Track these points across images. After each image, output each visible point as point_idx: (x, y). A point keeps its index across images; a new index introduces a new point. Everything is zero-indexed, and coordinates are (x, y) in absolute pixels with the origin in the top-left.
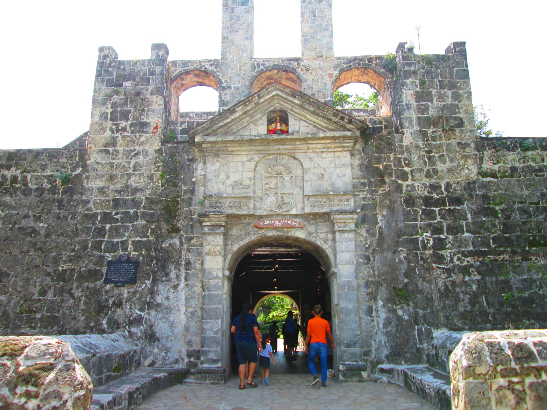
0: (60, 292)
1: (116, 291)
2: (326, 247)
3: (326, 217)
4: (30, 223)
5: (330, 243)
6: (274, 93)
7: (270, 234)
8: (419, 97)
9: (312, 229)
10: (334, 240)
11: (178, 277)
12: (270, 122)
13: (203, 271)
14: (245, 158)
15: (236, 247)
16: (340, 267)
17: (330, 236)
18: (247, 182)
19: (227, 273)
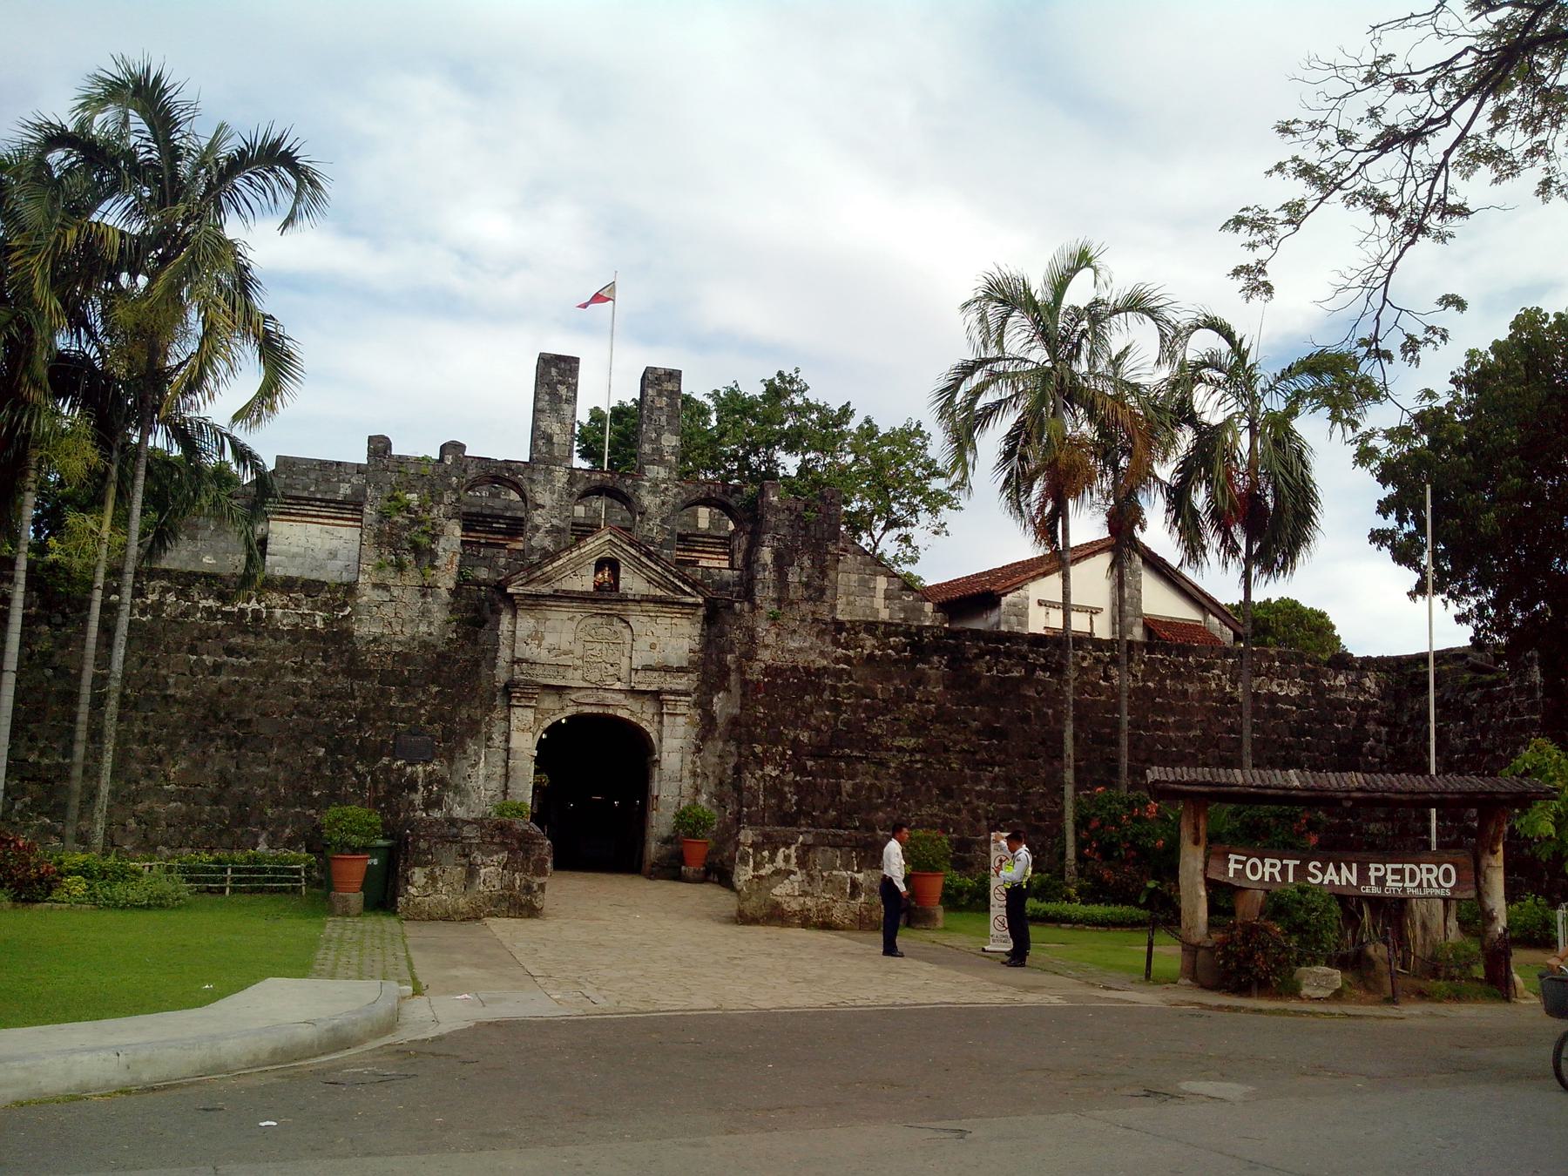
0: (338, 765)
1: (409, 769)
2: (652, 730)
3: (656, 696)
4: (290, 679)
5: (656, 725)
6: (609, 537)
7: (587, 710)
8: (778, 556)
9: (636, 707)
10: (661, 722)
11: (476, 754)
12: (600, 565)
13: (508, 750)
14: (565, 616)
15: (547, 723)
16: (665, 755)
17: (656, 718)
18: (565, 646)
19: (535, 753)
